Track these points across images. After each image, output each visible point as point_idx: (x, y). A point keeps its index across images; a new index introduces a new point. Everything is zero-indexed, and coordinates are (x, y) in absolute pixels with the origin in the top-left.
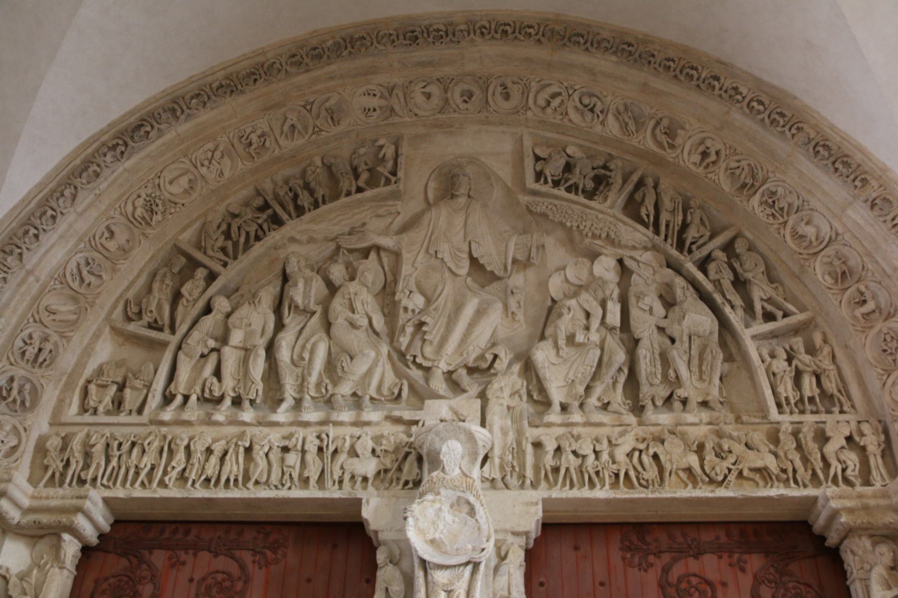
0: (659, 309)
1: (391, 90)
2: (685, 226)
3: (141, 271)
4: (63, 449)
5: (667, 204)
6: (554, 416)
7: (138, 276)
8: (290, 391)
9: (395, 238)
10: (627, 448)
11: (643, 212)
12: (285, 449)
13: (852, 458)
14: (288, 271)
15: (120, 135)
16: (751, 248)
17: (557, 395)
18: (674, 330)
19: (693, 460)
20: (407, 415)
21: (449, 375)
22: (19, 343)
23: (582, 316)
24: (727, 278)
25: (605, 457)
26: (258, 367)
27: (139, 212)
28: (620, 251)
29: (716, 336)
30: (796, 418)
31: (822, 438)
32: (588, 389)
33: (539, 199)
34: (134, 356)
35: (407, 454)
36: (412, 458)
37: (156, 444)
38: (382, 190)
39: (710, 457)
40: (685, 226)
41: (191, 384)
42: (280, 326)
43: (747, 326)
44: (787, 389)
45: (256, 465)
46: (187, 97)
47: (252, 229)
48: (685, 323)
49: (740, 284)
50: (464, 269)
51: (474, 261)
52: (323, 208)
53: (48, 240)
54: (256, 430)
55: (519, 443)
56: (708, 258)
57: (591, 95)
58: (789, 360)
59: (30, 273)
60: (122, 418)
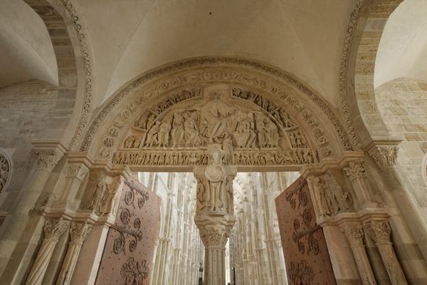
2: (269, 106)
5: (264, 101)
12: (174, 156)
13: (310, 158)
16: (284, 111)
17: (240, 144)
18: (267, 129)
19: (273, 158)
20: (204, 148)
24: (279, 118)
26: (167, 137)
28: (254, 112)
31: (303, 153)
34: (137, 134)
39: (277, 157)
40: (269, 106)
41: (150, 141)
42: (172, 128)
44: (294, 143)
49: (281, 119)
50: (216, 115)
51: (219, 113)
56: (274, 113)
60: (134, 149)
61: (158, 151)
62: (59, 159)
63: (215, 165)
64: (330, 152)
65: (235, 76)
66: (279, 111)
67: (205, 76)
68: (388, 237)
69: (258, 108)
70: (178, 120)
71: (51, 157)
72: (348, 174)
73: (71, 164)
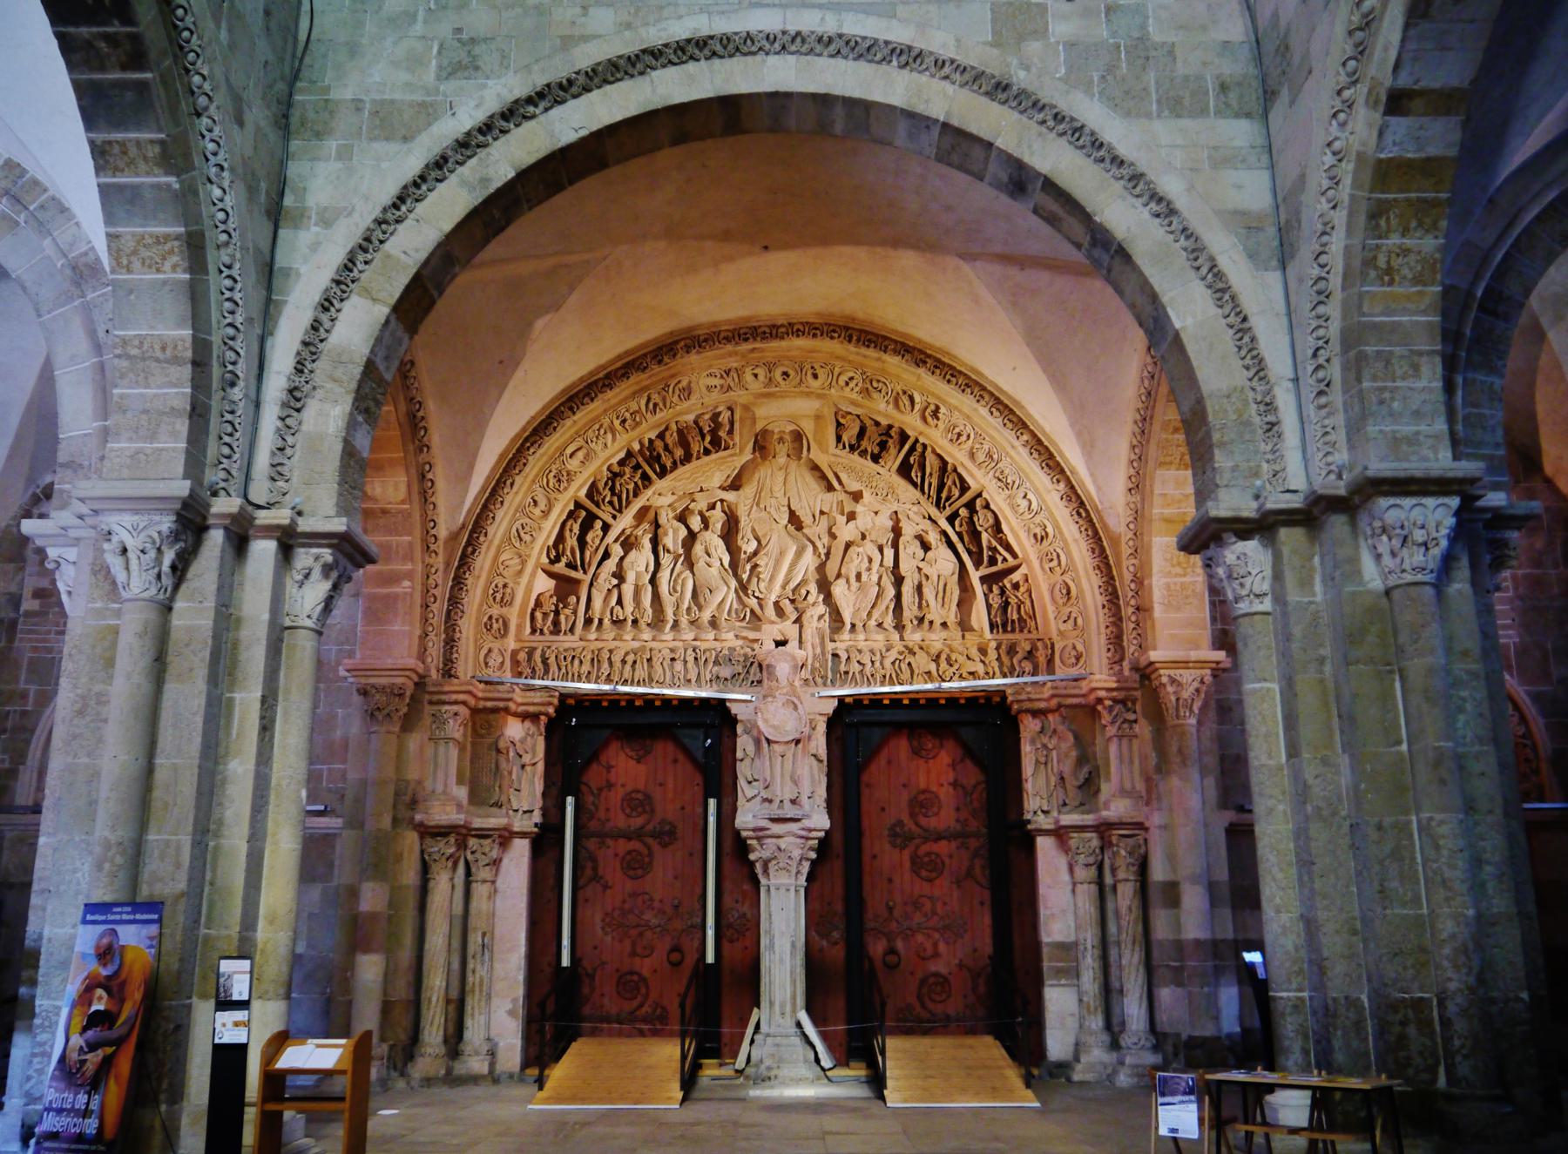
0: (921, 553)
1: (728, 373)
3: (555, 523)
4: (529, 660)
6: (845, 635)
7: (553, 527)
8: (670, 617)
9: (734, 493)
11: (913, 474)
12: (673, 659)
14: (660, 522)
15: (535, 432)
16: (987, 506)
19: (933, 667)
21: (776, 604)
22: (491, 592)
23: (866, 560)
25: (877, 664)
27: (552, 481)
29: (956, 576)
30: (1002, 636)
32: (869, 614)
33: (840, 460)
35: (752, 664)
36: (756, 665)
37: (589, 657)
38: (721, 454)
39: (944, 665)
41: (603, 613)
43: (977, 569)
45: (656, 672)
46: (581, 396)
47: (631, 487)
51: (792, 514)
52: (681, 470)
53: (498, 519)
55: (823, 653)
57: (878, 381)
58: (1003, 592)
59: (491, 541)
60: (561, 637)
61: (629, 640)
62: (407, 700)
63: (781, 699)
64: (1078, 658)
65: (844, 378)
66: (970, 506)
67: (748, 377)
68: (1135, 868)
70: (673, 537)
71: (397, 699)
72: (1103, 722)
73: (436, 707)
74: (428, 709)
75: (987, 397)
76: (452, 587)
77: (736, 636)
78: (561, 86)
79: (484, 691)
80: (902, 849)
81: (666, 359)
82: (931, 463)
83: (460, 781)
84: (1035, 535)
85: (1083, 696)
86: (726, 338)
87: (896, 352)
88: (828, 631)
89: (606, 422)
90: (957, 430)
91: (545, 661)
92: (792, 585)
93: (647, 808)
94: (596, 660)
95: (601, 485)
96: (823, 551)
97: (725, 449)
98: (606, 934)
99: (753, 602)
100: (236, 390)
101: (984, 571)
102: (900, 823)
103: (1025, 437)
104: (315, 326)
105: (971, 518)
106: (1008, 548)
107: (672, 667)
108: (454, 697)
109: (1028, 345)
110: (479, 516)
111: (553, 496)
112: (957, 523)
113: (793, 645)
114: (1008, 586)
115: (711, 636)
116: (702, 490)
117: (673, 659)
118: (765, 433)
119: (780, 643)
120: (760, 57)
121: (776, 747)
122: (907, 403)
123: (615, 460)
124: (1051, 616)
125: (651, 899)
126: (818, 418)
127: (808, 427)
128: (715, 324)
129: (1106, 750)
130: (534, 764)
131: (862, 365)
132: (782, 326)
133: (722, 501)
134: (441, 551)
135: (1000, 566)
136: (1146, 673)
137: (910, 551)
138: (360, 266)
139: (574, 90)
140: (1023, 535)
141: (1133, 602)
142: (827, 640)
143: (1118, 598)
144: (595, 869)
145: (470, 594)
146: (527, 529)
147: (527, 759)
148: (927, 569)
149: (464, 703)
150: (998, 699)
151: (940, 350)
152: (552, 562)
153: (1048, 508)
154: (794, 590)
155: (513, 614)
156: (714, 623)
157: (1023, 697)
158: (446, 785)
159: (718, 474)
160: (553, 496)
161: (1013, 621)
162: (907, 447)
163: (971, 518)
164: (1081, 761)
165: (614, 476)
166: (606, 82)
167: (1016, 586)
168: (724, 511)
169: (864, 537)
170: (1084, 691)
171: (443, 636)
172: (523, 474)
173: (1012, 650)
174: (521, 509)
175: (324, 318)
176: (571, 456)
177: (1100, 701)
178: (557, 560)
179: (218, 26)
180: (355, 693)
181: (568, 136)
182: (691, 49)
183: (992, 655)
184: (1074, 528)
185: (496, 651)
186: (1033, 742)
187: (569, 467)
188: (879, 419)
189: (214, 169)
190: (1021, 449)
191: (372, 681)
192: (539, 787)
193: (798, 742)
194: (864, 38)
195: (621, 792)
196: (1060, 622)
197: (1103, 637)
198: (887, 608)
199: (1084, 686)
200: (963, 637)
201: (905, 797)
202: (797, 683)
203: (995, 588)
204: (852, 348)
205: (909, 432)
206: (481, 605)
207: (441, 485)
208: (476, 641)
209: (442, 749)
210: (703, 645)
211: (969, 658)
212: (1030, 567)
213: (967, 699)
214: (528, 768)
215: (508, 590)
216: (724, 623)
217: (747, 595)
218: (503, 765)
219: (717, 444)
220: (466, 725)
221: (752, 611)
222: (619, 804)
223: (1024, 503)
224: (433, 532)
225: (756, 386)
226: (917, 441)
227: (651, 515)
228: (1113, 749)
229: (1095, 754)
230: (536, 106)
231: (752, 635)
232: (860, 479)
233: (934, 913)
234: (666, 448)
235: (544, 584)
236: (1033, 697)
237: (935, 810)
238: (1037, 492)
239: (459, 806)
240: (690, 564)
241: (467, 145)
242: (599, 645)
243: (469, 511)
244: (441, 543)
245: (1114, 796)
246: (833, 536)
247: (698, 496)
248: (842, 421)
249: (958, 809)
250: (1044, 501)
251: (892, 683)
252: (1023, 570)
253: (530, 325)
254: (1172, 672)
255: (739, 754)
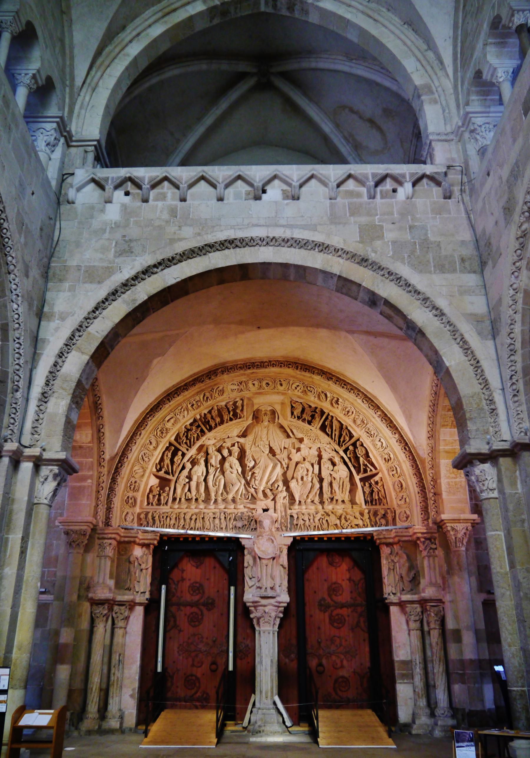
0: (331, 467)
1: (241, 383)
6: (296, 507)
8: (213, 498)
10: (318, 518)
12: (214, 518)
15: (152, 410)
16: (362, 445)
19: (338, 522)
21: (263, 491)
23: (306, 470)
25: (312, 521)
27: (159, 433)
29: (348, 479)
32: (308, 496)
37: (174, 516)
39: (343, 521)
41: (181, 495)
47: (196, 436)
48: (340, 473)
51: (271, 448)
52: (219, 428)
53: (133, 451)
54: (205, 511)
55: (286, 515)
58: (370, 485)
60: (161, 507)
62: (87, 537)
63: (266, 537)
65: (294, 386)
66: (354, 445)
67: (250, 385)
69: (325, 438)
73: (102, 541)
74: (97, 542)
75: (361, 395)
76: (111, 483)
77: (245, 507)
78: (169, 260)
79: (124, 533)
80: (324, 612)
81: (213, 377)
82: (335, 424)
83: (111, 577)
84: (385, 459)
85: (410, 536)
86: (240, 368)
87: (318, 374)
88: (288, 505)
89: (184, 405)
90: (347, 410)
91: (153, 518)
92: (271, 482)
93: (201, 591)
94: (177, 518)
95: (181, 435)
96: (285, 466)
97: (240, 418)
98: (180, 655)
99: (252, 490)
100: (18, 393)
101: (362, 476)
102: (323, 599)
103: (379, 413)
104: (55, 365)
105: (355, 451)
106: (373, 464)
107: (214, 522)
108: (110, 536)
109: (379, 371)
110: (125, 449)
111: (159, 440)
112: (348, 453)
113: (271, 511)
114: (373, 483)
115: (232, 506)
116: (228, 437)
117: (214, 518)
118: (258, 410)
119: (266, 510)
120: (257, 248)
121: (263, 561)
122: (324, 397)
123: (188, 423)
124: (394, 497)
125: (202, 638)
126: (283, 404)
127: (278, 408)
128: (235, 361)
129: (422, 563)
130: (147, 569)
131: (303, 380)
132: (266, 362)
133: (238, 442)
134: (106, 466)
135: (369, 473)
136: (440, 525)
137: (326, 466)
138: (77, 338)
139: (175, 261)
140: (379, 459)
141: (432, 491)
142: (288, 509)
143: (425, 489)
144: (175, 621)
145: (119, 486)
146: (147, 455)
147: (143, 566)
148: (334, 475)
149: (114, 539)
150: (369, 538)
151: (338, 373)
152: (158, 471)
153: (391, 446)
154: (272, 485)
155: (139, 496)
156: (234, 500)
157: (382, 536)
158: (104, 579)
159: (236, 430)
160: (159, 440)
161: (376, 500)
162: (324, 417)
163: (355, 451)
164: (411, 567)
165: (188, 430)
166: (189, 258)
167: (377, 483)
168: (239, 447)
169: (304, 459)
170: (411, 534)
171: (106, 506)
172: (146, 429)
173: (375, 514)
174: (144, 446)
175: (60, 361)
176: (168, 421)
177: (418, 538)
178: (160, 470)
179: (20, 237)
180: (63, 534)
181: (171, 281)
182: (226, 244)
183: (366, 516)
184: (403, 455)
185: (130, 513)
186: (387, 559)
187: (167, 427)
188: (311, 404)
189: (15, 296)
190: (377, 418)
191: (71, 528)
192: (149, 580)
193: (274, 559)
194: (303, 240)
195: (187, 584)
196: (398, 500)
197: (419, 508)
198: (316, 493)
199: (411, 531)
200: (352, 507)
201: (326, 586)
202: (274, 530)
203: (367, 484)
204: (298, 372)
205: (325, 411)
206: (124, 491)
207: (107, 434)
208: (121, 508)
209: (103, 561)
210: (229, 511)
211: (355, 518)
212: (383, 473)
213: (355, 538)
214: (144, 571)
215: (137, 484)
216: (238, 501)
217: (250, 487)
218: (132, 569)
219: (236, 416)
220: (115, 549)
221: (252, 495)
222: (187, 589)
223: (380, 444)
224: (103, 457)
225: (253, 389)
226: (329, 414)
227: (204, 449)
228: (426, 563)
229: (417, 565)
230: (158, 268)
231: (252, 506)
232: (302, 432)
233: (341, 645)
234: (212, 418)
235: (154, 481)
236: (387, 536)
237: (340, 592)
238: (385, 439)
239: (110, 589)
240: (223, 472)
241: (126, 285)
242: (179, 511)
243: (120, 447)
244: (106, 462)
245: (427, 586)
246: (290, 459)
247: (226, 440)
248: (294, 405)
249: (351, 592)
250: (389, 443)
251: (319, 530)
252: (380, 475)
253: (151, 362)
254: (452, 525)
255: (246, 564)
